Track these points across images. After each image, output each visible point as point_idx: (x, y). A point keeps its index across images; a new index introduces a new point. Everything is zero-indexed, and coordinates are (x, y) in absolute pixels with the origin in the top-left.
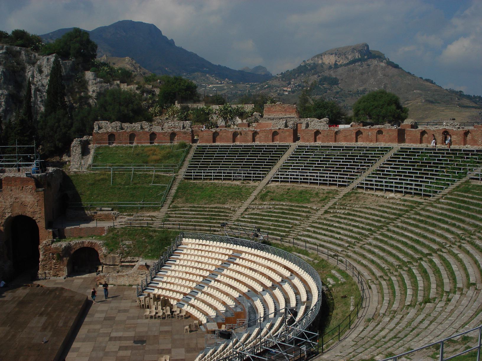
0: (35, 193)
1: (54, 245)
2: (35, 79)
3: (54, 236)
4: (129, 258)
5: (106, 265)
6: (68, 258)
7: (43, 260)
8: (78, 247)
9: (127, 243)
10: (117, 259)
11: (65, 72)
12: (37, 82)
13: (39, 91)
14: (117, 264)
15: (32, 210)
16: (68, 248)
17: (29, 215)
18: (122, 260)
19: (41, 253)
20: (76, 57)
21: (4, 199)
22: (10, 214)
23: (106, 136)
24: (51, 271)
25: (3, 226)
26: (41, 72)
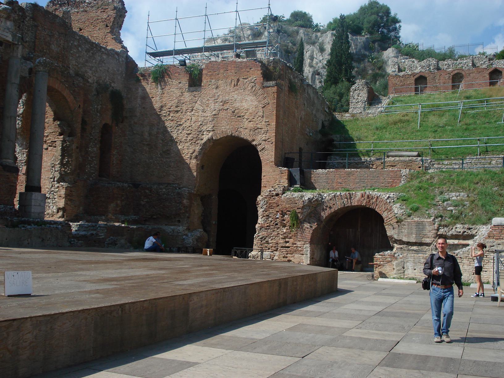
0: (260, 92)
1: (288, 194)
2: (315, 60)
3: (292, 181)
4: (459, 228)
5: (401, 242)
6: (315, 226)
7: (261, 228)
8: (338, 205)
9: (454, 196)
10: (428, 228)
11: (356, 49)
12: (317, 64)
13: (319, 74)
14: (428, 241)
15: (251, 125)
16: (315, 206)
17: (245, 135)
18: (441, 231)
19: (260, 211)
20: (371, 33)
21: (202, 104)
22: (211, 134)
23: (412, 80)
24: (277, 253)
25: (196, 157)
26: (322, 50)
